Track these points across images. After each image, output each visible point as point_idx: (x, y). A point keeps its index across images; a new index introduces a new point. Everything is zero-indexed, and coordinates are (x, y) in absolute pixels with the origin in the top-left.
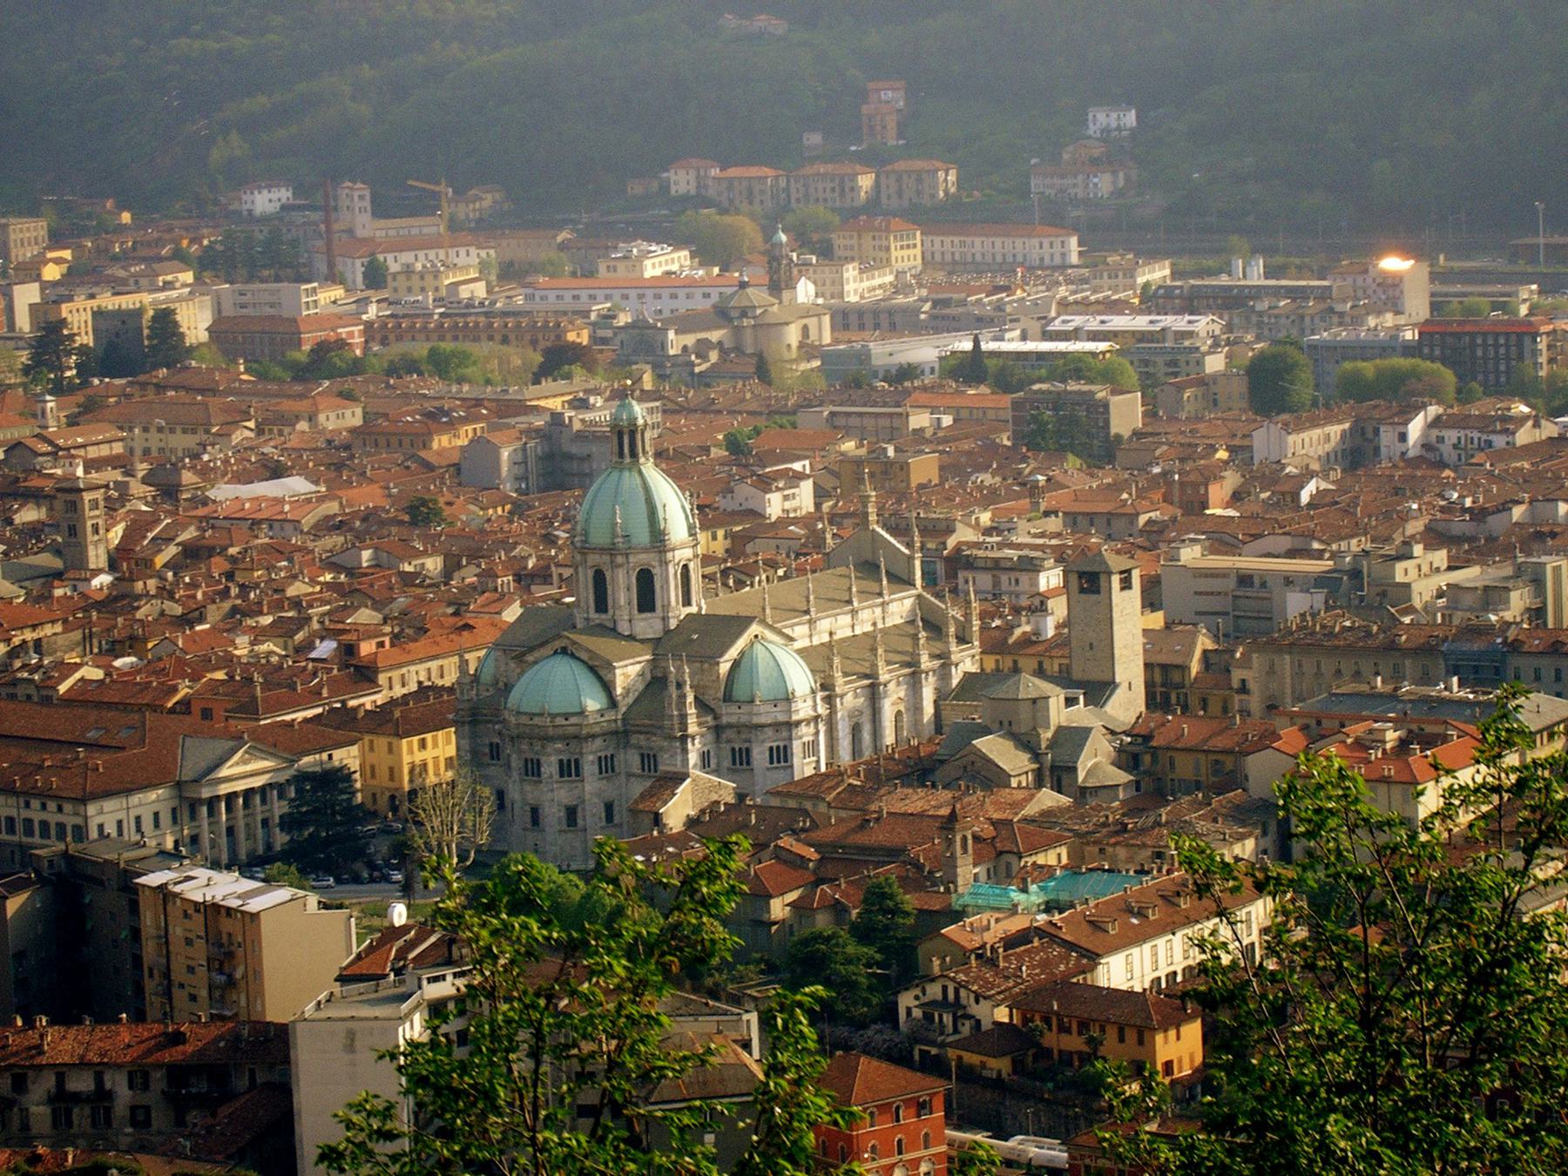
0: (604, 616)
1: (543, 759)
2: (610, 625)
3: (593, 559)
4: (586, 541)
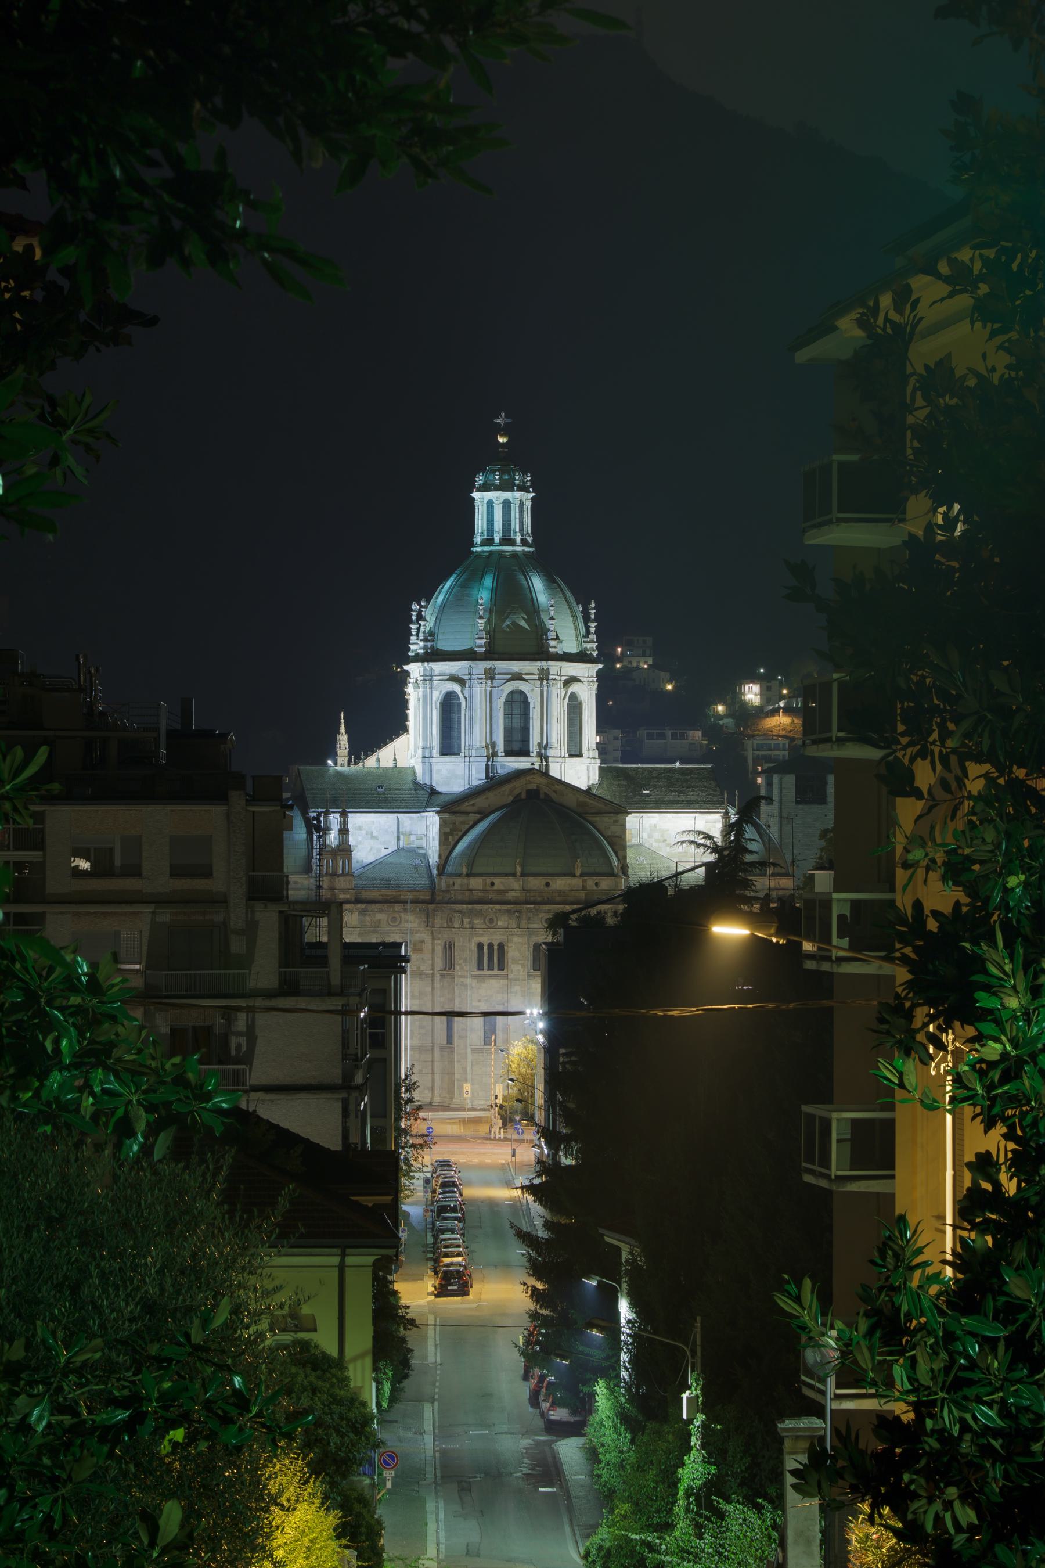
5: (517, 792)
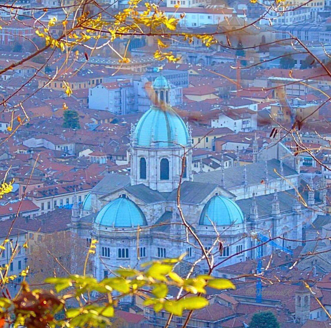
0: (144, 180)
1: (111, 248)
2: (147, 185)
3: (140, 152)
4: (137, 144)
5: (120, 195)
